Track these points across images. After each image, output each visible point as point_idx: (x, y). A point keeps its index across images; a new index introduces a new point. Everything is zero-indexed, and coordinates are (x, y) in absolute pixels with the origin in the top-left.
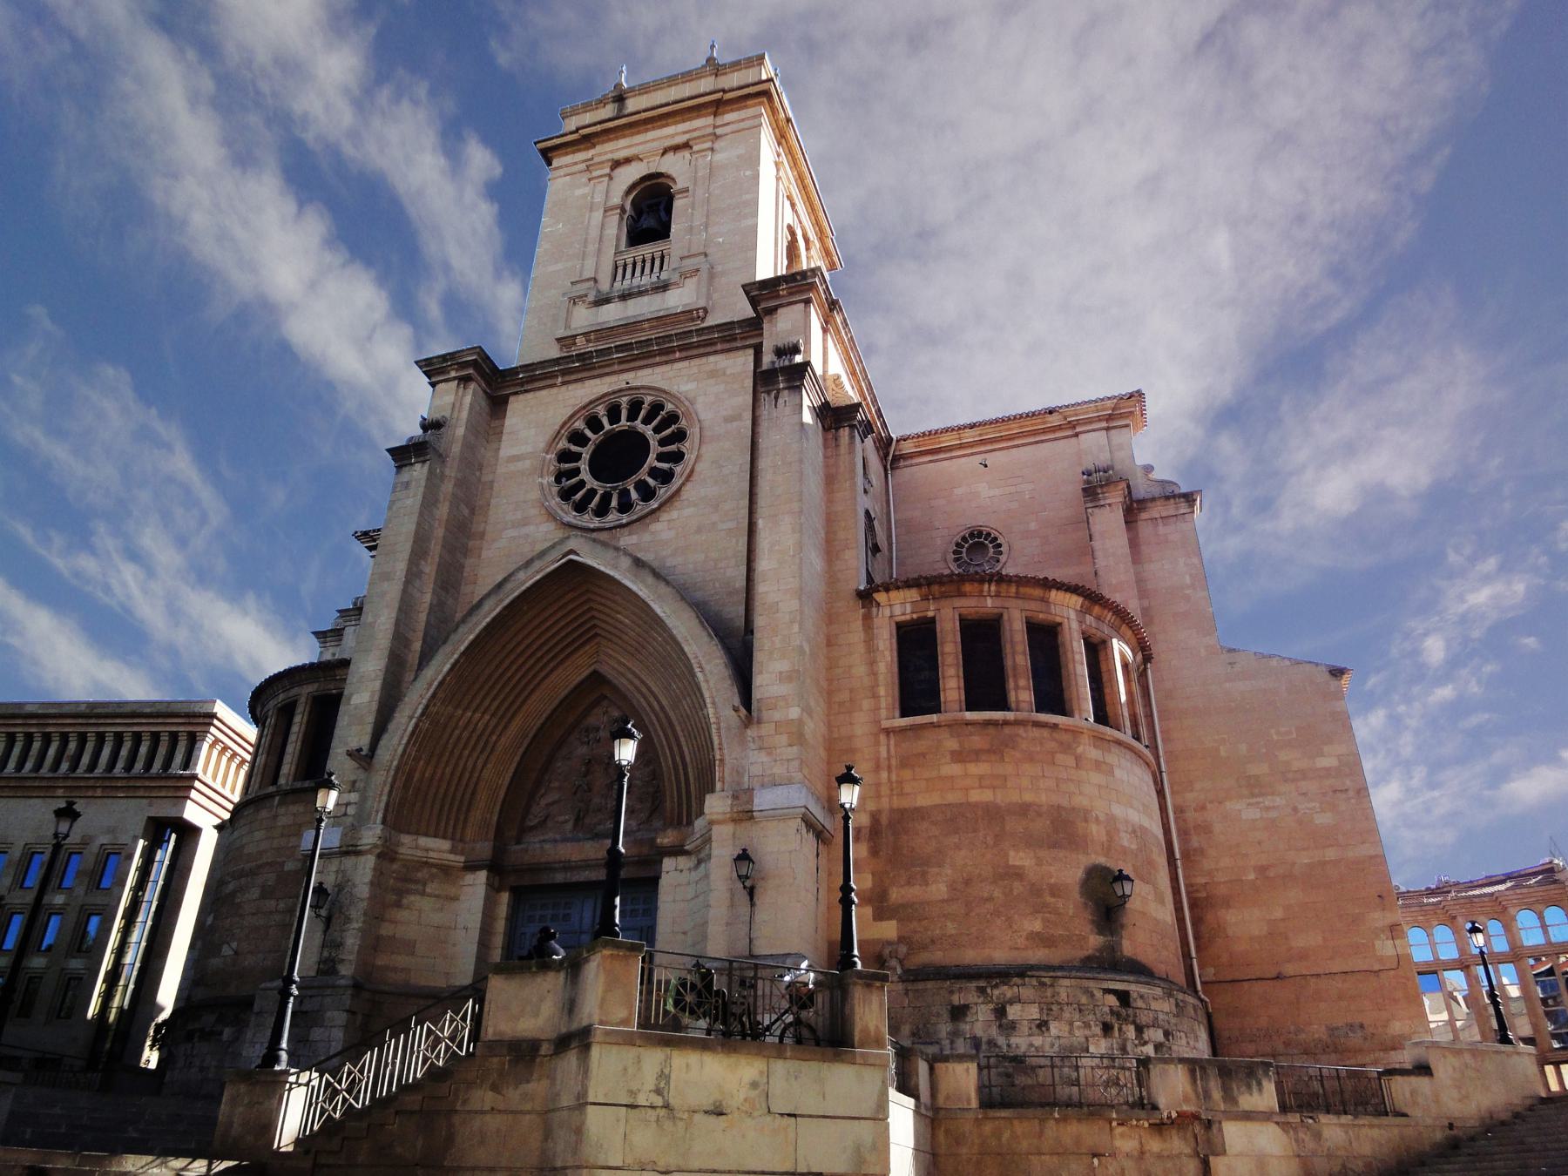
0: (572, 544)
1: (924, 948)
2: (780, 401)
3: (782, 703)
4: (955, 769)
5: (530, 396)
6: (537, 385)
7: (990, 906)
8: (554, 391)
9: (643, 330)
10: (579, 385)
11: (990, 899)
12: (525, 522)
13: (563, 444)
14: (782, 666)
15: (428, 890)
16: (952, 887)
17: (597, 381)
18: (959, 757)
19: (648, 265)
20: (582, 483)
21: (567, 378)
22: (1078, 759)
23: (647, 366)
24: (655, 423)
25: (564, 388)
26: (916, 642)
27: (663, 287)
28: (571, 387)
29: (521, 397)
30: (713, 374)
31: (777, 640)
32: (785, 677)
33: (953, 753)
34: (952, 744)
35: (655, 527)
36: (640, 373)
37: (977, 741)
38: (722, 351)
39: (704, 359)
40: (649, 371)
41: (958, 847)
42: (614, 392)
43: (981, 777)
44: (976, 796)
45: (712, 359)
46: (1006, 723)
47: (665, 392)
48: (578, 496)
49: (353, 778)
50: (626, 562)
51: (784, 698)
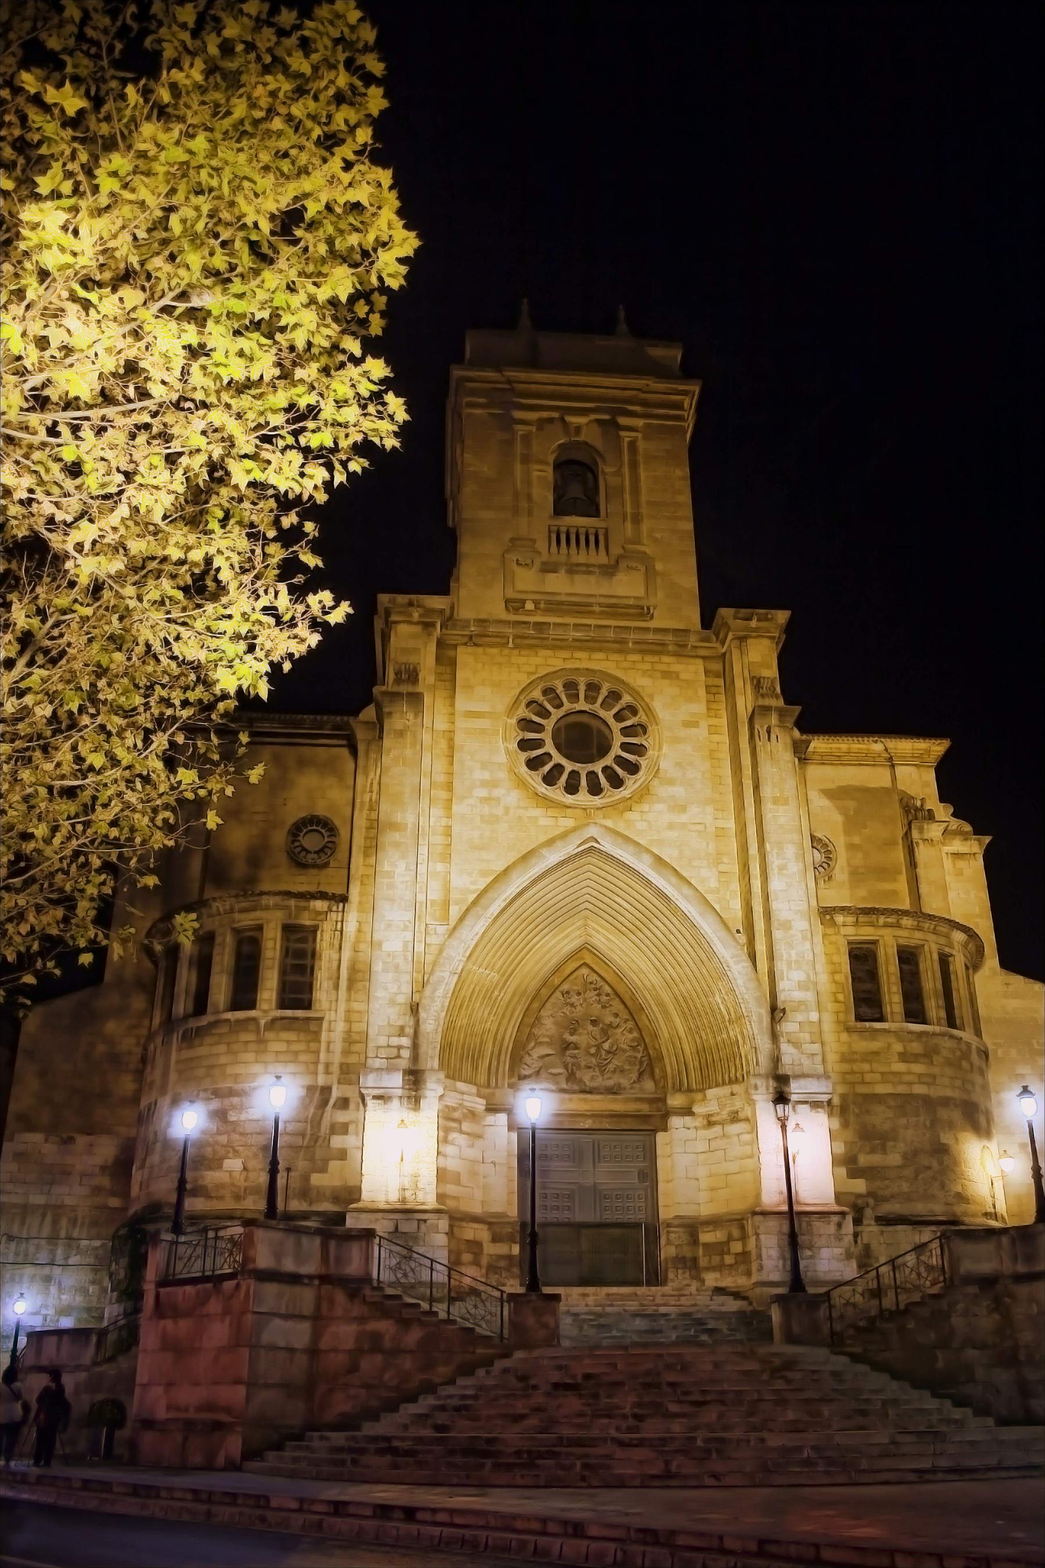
0: (593, 831)
1: (886, 1200)
2: (773, 737)
3: (803, 1007)
4: (899, 1067)
5: (480, 650)
7: (930, 1173)
8: (506, 651)
11: (929, 1168)
12: (492, 784)
13: (522, 712)
14: (798, 976)
16: (905, 1156)
18: (904, 1057)
20: (548, 755)
22: (972, 1065)
25: (516, 652)
26: (862, 959)
27: (609, 571)
29: (470, 649)
30: (666, 675)
31: (793, 953)
32: (802, 986)
33: (900, 1054)
34: (898, 1047)
35: (629, 815)
37: (916, 1047)
40: (601, 655)
41: (906, 1128)
43: (920, 1075)
44: (919, 1089)
45: (666, 659)
46: (934, 1034)
47: (623, 682)
49: (400, 1023)
50: (647, 858)
51: (801, 1003)
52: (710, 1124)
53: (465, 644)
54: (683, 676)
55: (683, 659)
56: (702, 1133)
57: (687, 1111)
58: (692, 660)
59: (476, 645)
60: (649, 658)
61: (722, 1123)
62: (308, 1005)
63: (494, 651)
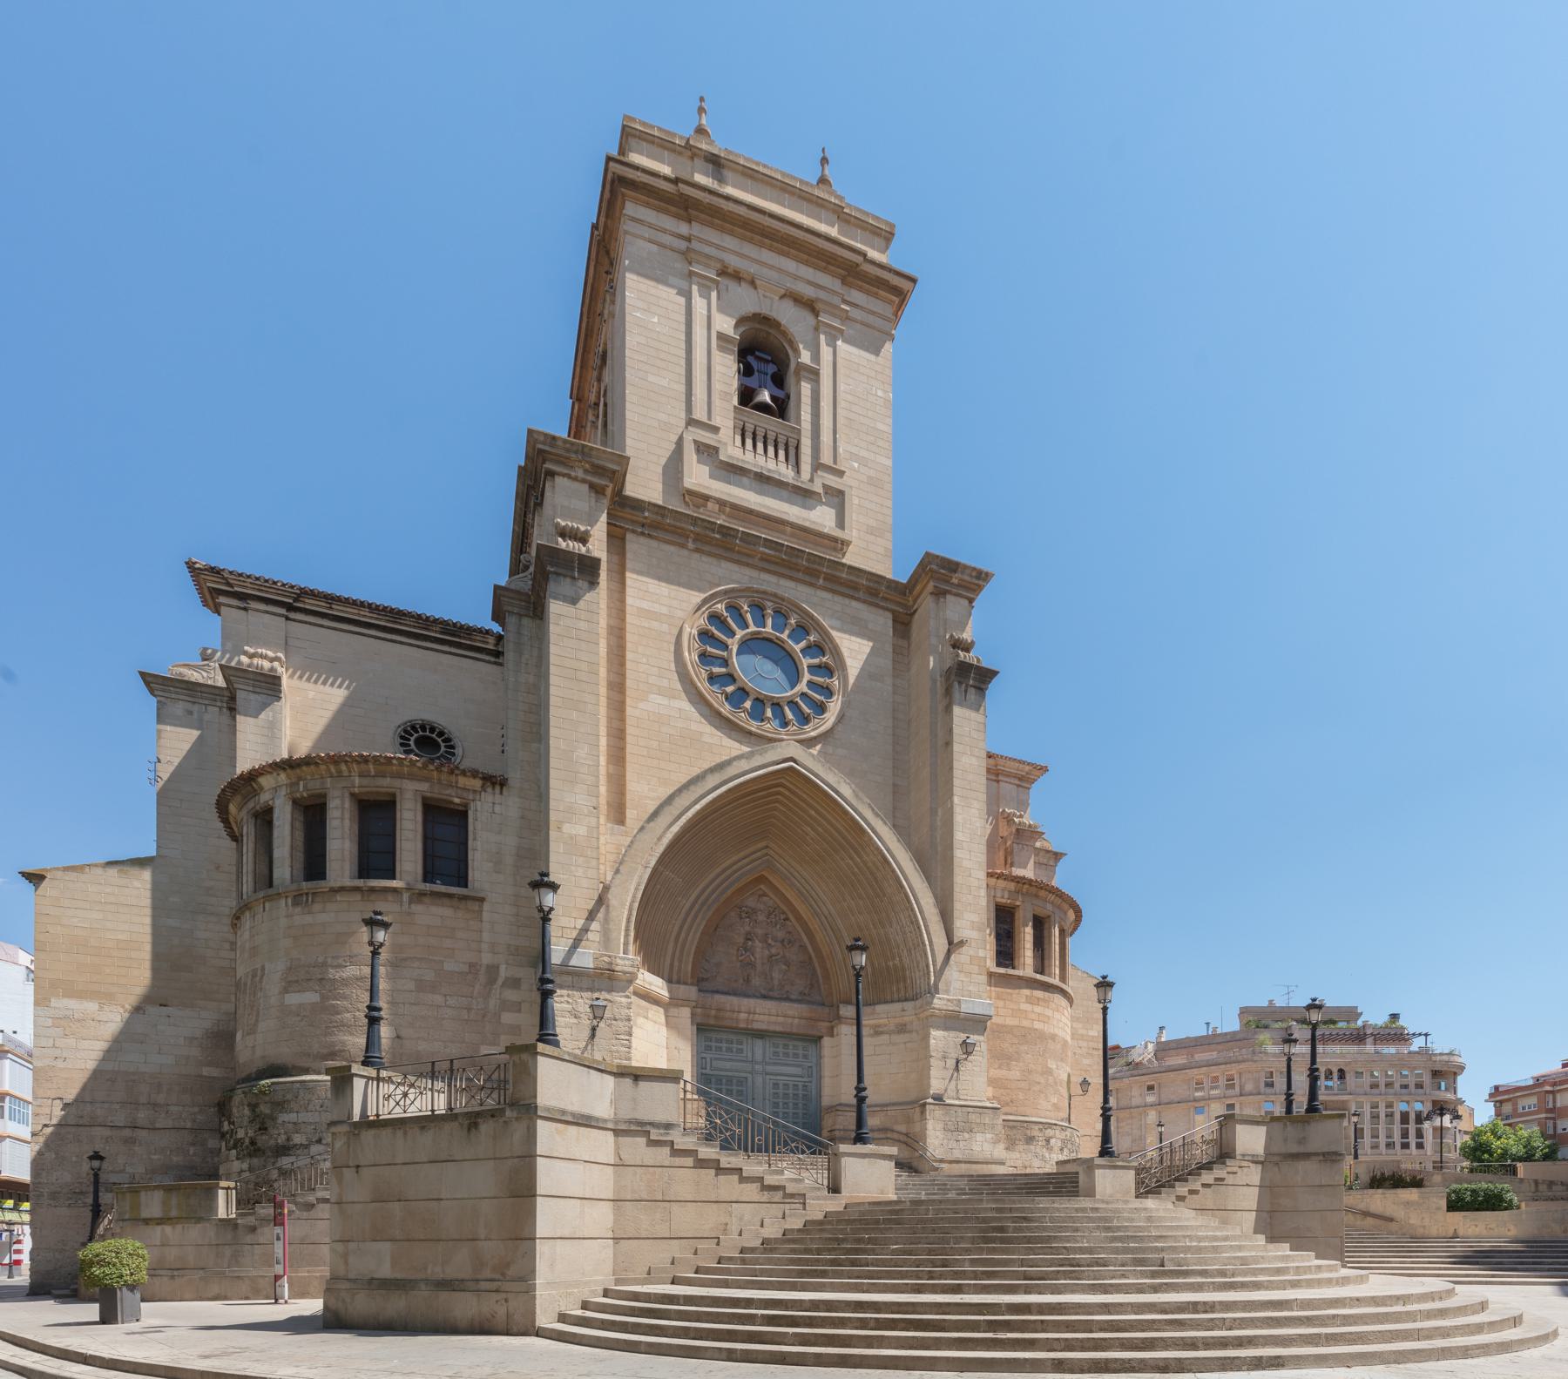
5: (654, 543)
6: (661, 534)
8: (685, 552)
9: (783, 532)
17: (735, 567)
19: (771, 450)
21: (699, 545)
23: (791, 578)
25: (697, 556)
28: (705, 558)
29: (642, 540)
36: (783, 582)
42: (757, 591)
53: (634, 532)
59: (650, 536)
63: (672, 548)
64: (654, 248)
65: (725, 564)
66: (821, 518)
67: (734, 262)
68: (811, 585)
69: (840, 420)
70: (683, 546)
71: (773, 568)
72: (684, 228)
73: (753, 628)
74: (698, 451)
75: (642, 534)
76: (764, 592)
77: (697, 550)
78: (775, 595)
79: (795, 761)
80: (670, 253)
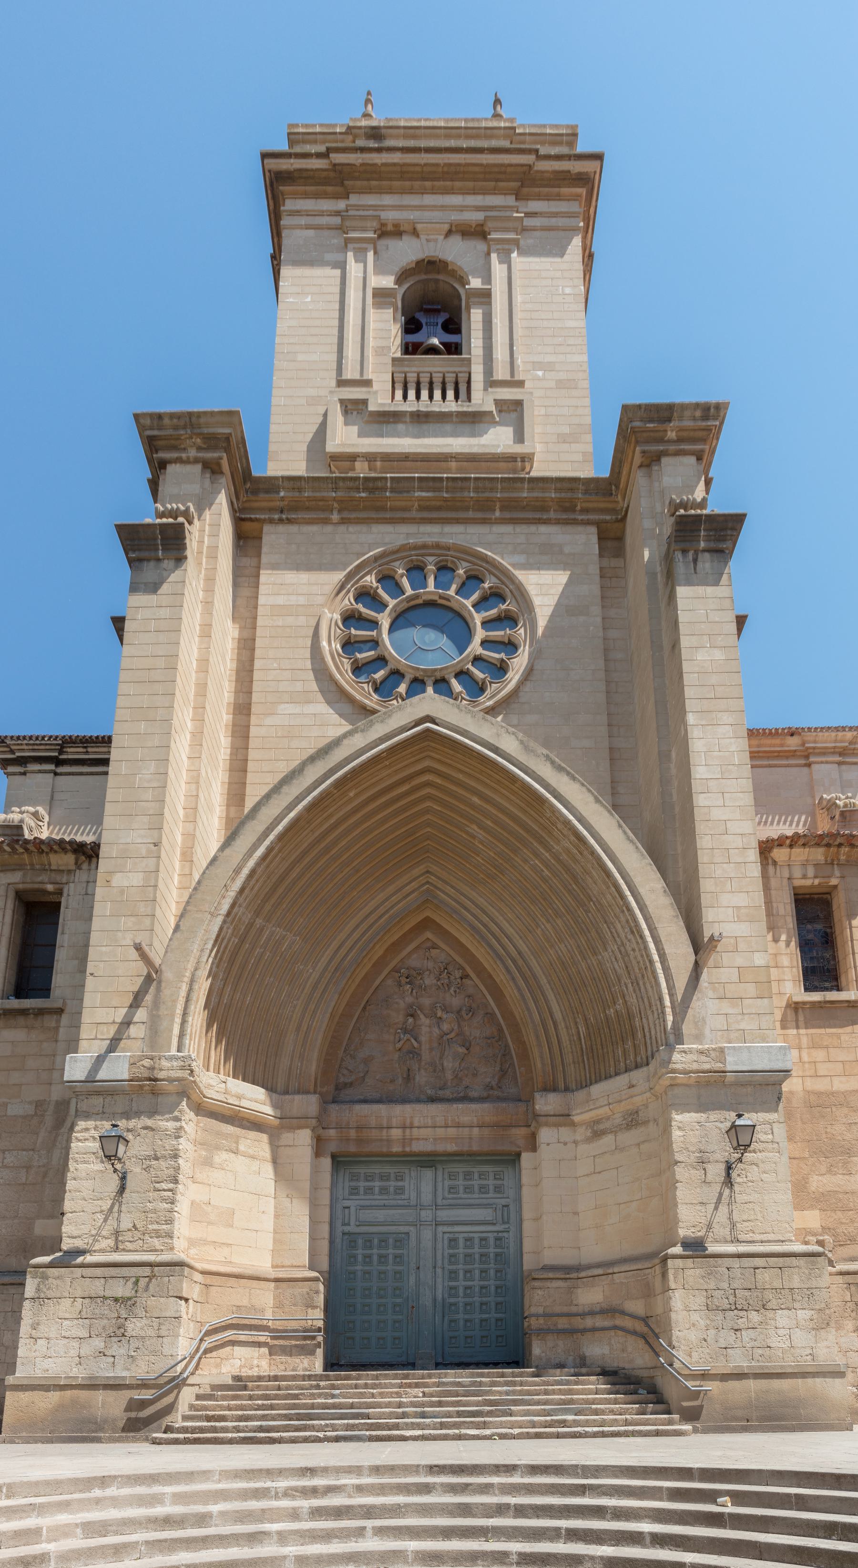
5: (294, 528)
6: (300, 515)
8: (329, 528)
10: (364, 528)
15: (242, 1148)
21: (346, 515)
23: (458, 521)
24: (475, 596)
25: (342, 528)
28: (352, 528)
29: (281, 528)
36: (448, 529)
38: (558, 522)
39: (533, 528)
42: (416, 547)
45: (543, 529)
48: (379, 675)
52: (597, 1134)
53: (271, 521)
54: (567, 549)
55: (569, 528)
56: (583, 1148)
57: (564, 1118)
58: (580, 528)
60: (520, 529)
61: (614, 1131)
62: (45, 991)
63: (314, 528)
64: (311, 233)
65: (377, 529)
66: (497, 439)
67: (390, 216)
68: (484, 521)
69: (518, 332)
70: (326, 521)
71: (435, 515)
72: (341, 205)
73: (409, 592)
74: (346, 412)
75: (281, 521)
76: (424, 546)
77: (344, 521)
78: (437, 546)
79: (433, 720)
80: (326, 233)
